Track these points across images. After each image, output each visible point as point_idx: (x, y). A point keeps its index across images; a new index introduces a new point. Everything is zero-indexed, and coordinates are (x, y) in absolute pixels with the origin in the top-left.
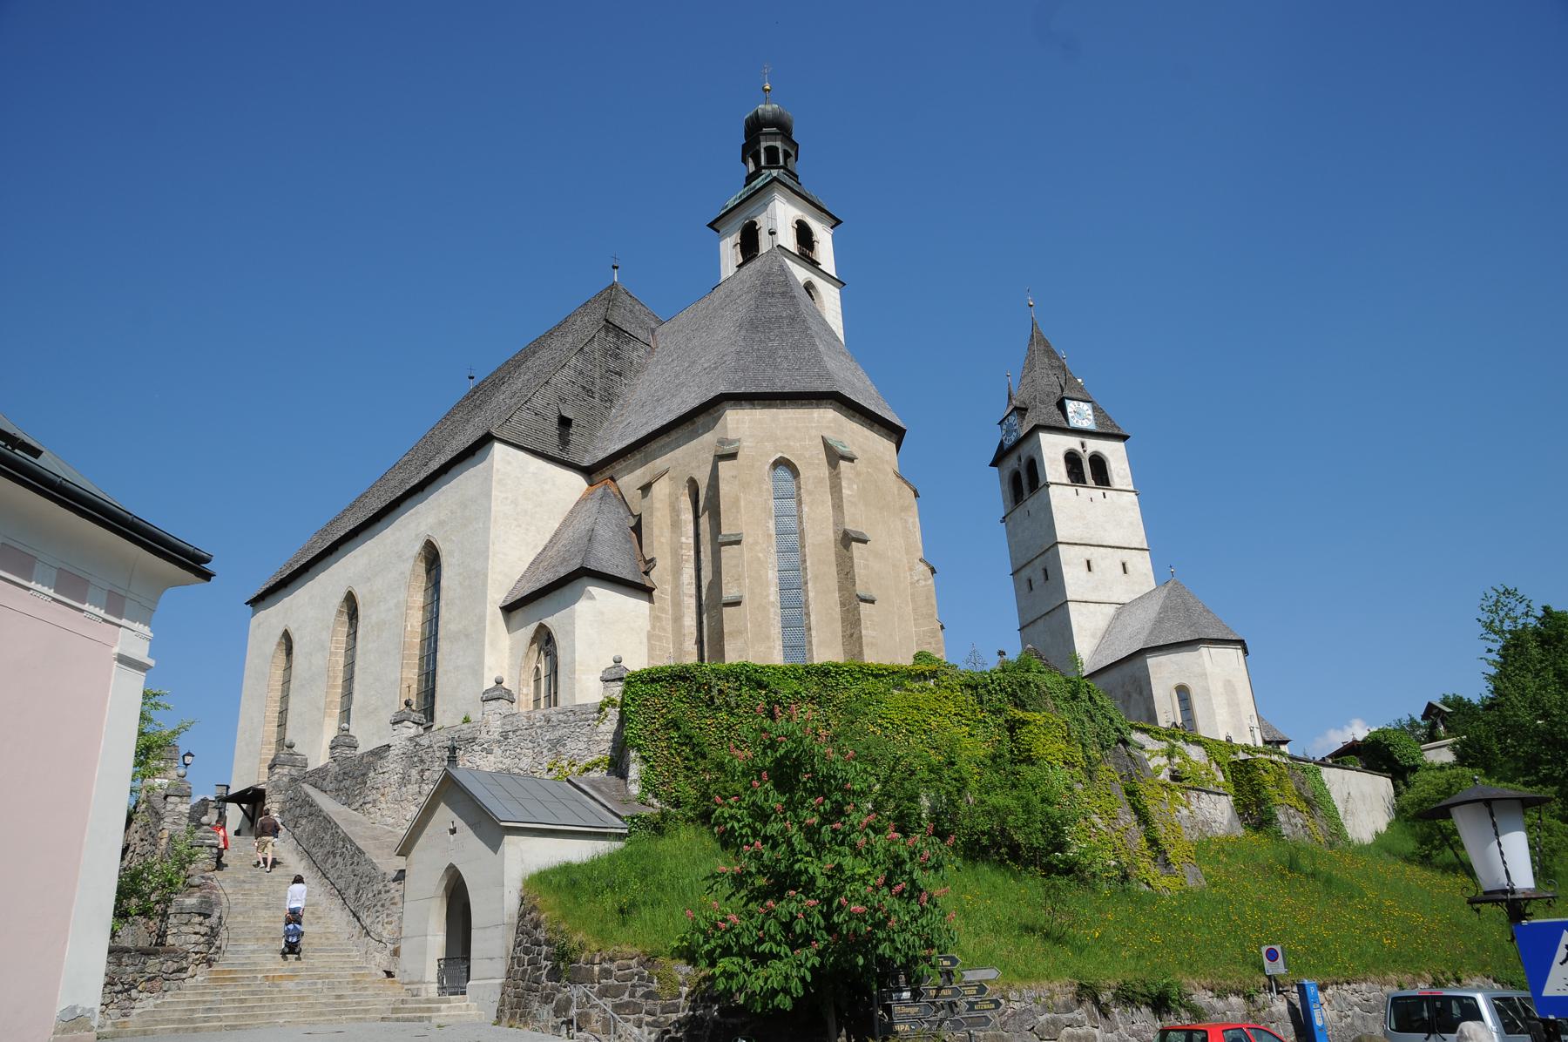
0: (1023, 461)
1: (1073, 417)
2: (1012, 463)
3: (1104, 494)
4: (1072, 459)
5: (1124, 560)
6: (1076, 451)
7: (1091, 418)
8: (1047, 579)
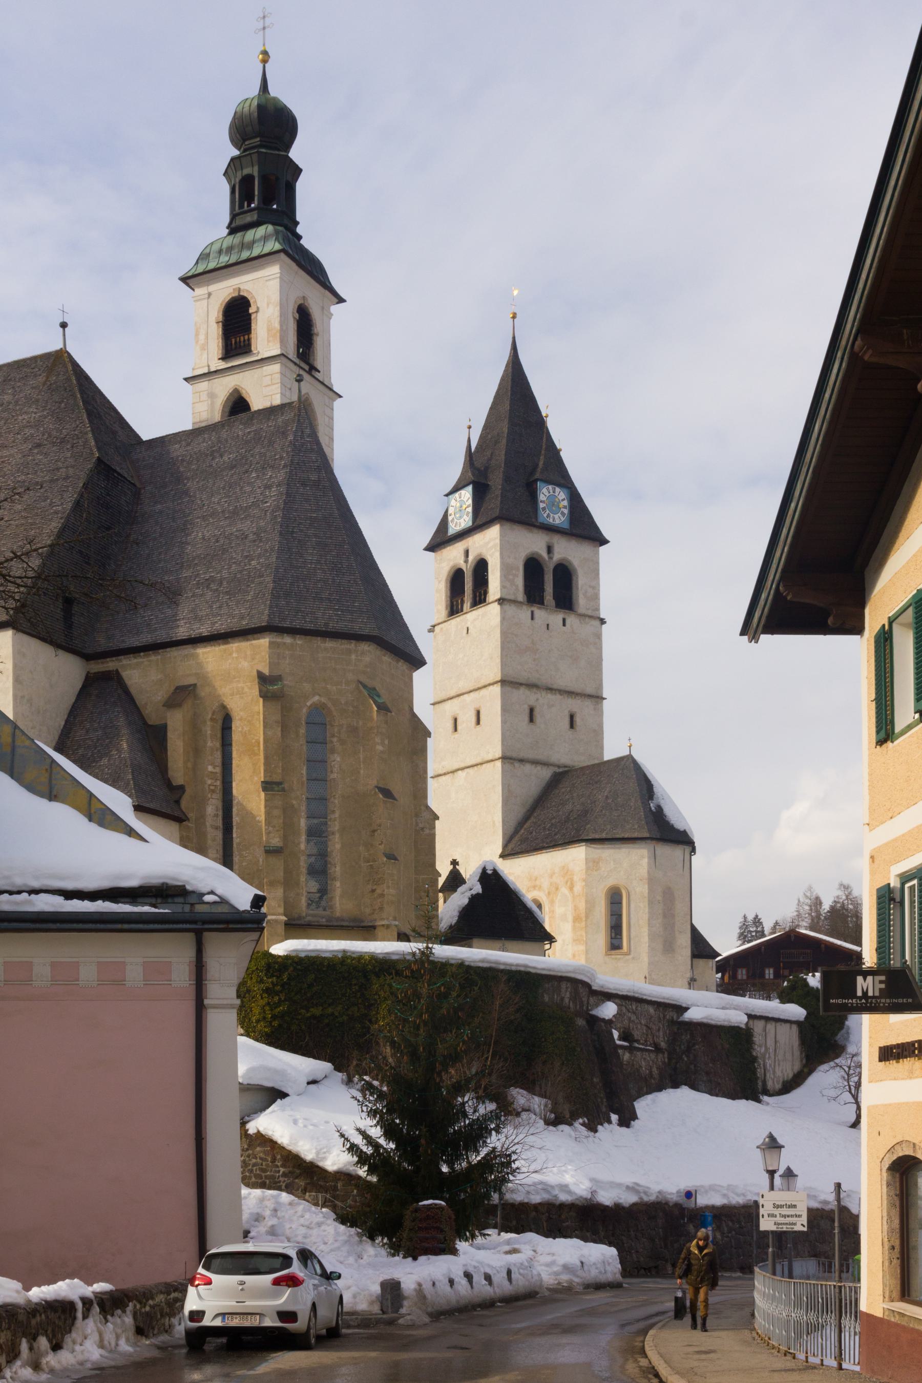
0: (471, 558)
1: (544, 509)
2: (453, 556)
3: (564, 620)
4: (533, 567)
5: (574, 710)
6: (541, 556)
7: (566, 511)
8: (478, 722)
